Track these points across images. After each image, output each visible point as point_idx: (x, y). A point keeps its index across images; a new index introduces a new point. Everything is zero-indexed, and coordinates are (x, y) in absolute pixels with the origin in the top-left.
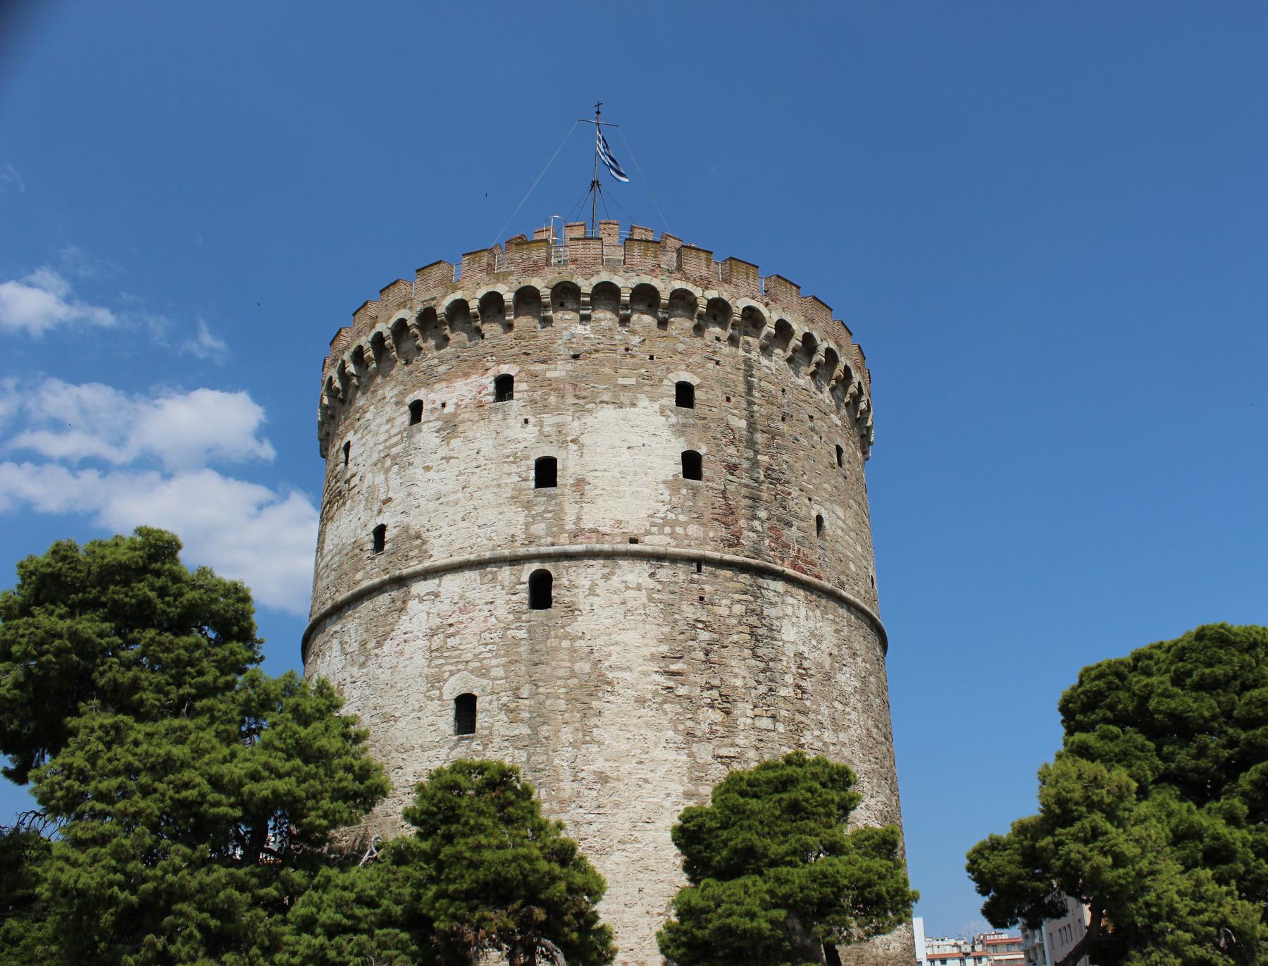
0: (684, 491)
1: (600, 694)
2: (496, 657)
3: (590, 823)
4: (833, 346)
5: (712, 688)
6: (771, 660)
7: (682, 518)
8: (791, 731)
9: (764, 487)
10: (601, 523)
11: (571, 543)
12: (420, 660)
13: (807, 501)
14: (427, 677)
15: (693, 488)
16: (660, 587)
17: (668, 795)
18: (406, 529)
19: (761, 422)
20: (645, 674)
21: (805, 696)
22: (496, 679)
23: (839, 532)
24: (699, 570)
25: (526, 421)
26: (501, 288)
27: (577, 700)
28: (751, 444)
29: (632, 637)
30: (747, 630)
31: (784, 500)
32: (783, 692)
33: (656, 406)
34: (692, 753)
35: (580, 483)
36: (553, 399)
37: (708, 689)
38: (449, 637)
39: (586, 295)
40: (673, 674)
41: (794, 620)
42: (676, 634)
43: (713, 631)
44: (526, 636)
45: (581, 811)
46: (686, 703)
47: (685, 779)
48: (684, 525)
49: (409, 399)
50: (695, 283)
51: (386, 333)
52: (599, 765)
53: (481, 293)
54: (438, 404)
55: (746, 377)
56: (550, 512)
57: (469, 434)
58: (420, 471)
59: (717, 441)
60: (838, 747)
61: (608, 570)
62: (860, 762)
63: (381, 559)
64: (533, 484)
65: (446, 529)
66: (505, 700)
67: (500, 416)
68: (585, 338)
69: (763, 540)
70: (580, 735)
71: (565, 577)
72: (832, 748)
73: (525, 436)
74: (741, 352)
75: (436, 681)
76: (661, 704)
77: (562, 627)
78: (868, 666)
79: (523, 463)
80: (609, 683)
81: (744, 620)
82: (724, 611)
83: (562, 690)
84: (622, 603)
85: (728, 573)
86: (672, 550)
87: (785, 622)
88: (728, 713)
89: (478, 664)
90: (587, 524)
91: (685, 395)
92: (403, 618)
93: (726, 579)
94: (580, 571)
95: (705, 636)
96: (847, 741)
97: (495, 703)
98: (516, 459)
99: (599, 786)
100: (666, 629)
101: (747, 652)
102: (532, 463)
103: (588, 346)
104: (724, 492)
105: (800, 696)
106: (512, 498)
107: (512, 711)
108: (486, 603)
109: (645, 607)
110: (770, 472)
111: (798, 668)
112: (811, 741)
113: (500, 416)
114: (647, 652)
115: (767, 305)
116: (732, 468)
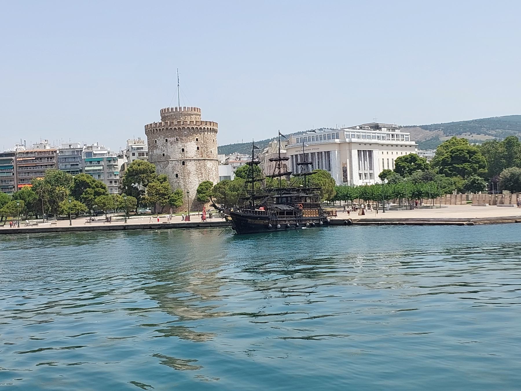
4: (213, 127)
12: (171, 170)
15: (198, 151)
26: (176, 127)
28: (204, 144)
29: (193, 168)
35: (187, 151)
36: (183, 141)
49: (166, 138)
51: (161, 129)
52: (190, 181)
53: (174, 127)
63: (164, 158)
71: (186, 162)
75: (173, 172)
91: (197, 140)
95: (200, 167)
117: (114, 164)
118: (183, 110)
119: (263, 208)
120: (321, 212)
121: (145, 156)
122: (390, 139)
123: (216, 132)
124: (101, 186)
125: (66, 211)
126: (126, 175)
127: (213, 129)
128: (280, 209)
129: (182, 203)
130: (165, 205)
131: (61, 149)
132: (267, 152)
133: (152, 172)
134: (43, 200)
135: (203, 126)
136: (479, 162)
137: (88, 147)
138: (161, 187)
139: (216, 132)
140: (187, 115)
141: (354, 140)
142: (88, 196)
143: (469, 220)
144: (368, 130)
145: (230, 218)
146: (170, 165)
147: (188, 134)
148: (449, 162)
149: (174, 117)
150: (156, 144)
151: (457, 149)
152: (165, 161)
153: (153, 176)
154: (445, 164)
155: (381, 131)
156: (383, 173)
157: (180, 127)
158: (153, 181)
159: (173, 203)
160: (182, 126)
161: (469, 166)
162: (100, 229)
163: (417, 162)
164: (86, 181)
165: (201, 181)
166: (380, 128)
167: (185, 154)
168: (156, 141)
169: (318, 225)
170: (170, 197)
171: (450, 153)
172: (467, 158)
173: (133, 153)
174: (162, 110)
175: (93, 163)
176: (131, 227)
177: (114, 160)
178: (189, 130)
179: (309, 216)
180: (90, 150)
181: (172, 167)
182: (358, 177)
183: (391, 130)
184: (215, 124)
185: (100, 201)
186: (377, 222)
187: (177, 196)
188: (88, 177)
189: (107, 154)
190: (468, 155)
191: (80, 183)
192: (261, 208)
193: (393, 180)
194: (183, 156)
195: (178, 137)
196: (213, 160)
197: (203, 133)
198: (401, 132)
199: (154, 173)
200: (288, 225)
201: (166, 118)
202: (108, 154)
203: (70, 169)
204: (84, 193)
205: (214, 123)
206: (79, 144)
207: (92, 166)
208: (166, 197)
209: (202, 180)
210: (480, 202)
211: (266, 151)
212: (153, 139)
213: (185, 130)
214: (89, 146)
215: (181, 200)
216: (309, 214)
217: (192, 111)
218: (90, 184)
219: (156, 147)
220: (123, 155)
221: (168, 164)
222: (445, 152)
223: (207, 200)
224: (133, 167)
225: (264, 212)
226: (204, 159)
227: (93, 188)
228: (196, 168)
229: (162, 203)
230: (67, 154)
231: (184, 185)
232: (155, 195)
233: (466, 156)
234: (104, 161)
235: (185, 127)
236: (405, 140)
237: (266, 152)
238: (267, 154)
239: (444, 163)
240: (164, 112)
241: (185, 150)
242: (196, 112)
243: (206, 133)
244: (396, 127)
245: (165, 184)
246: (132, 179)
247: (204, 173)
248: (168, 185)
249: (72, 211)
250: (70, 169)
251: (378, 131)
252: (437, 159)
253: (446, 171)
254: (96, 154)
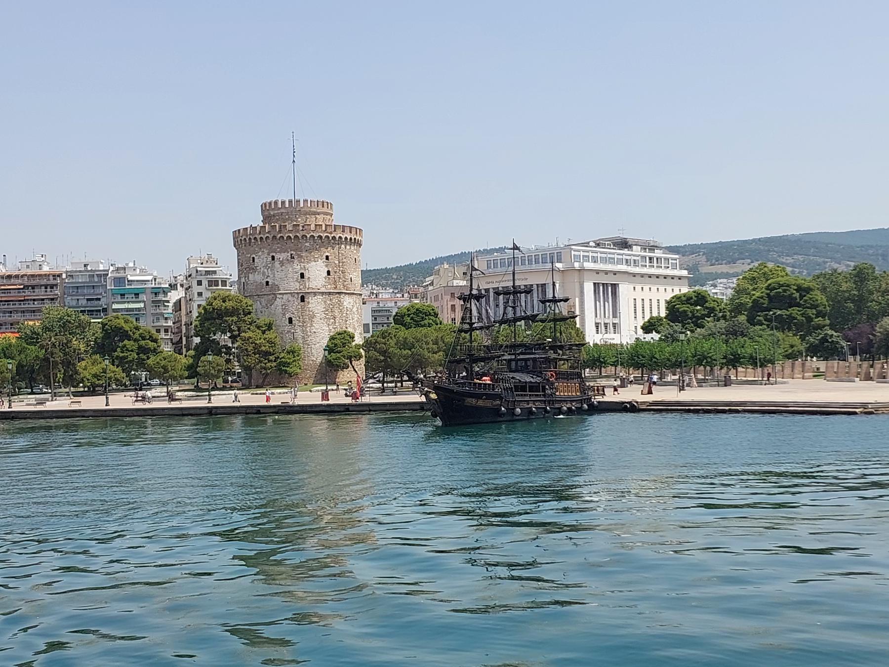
4: (355, 237)
12: (281, 310)
26: (291, 235)
35: (309, 278)
36: (303, 260)
49: (271, 254)
51: (264, 238)
52: (314, 330)
53: (287, 235)
63: (268, 288)
75: (284, 314)
91: (327, 258)
95: (331, 306)
116: (336, 272)
117: (163, 299)
118: (302, 205)
119: (488, 378)
120: (583, 389)
121: (220, 287)
122: (646, 266)
123: (358, 244)
124: (150, 337)
125: (88, 380)
126: (199, 318)
127: (355, 239)
128: (520, 381)
129: (300, 369)
130: (269, 371)
131: (70, 272)
132: (432, 284)
133: (248, 314)
134: (52, 359)
135: (337, 234)
136: (817, 306)
137: (118, 269)
138: (262, 340)
139: (358, 244)
140: (309, 215)
141: (588, 265)
142: (126, 354)
143: (864, 405)
144: (609, 248)
145: (433, 396)
146: (278, 302)
147: (312, 248)
148: (765, 306)
149: (287, 217)
150: (254, 264)
151: (779, 284)
152: (270, 294)
153: (249, 320)
154: (757, 309)
155: (632, 251)
156: (649, 321)
157: (298, 234)
158: (249, 329)
159: (284, 368)
160: (302, 233)
161: (799, 313)
162: (164, 413)
163: (707, 305)
164: (123, 327)
165: (333, 330)
166: (630, 246)
167: (305, 284)
168: (253, 258)
169: (580, 411)
170: (279, 357)
171: (766, 289)
172: (796, 299)
173: (198, 281)
174: (265, 204)
175: (126, 297)
176: (222, 411)
177: (164, 291)
178: (314, 240)
179: (566, 394)
180: (121, 274)
181: (282, 306)
182: (594, 329)
183: (647, 250)
184: (358, 230)
185: (157, 363)
186: (687, 408)
187: (291, 356)
188: (126, 322)
189: (152, 281)
190: (798, 294)
191: (113, 331)
192: (484, 378)
193: (669, 334)
194: (301, 287)
195: (294, 253)
196: (353, 294)
197: (338, 246)
198: (663, 253)
199: (250, 315)
200: (534, 409)
201: (273, 218)
202: (153, 282)
203: (85, 307)
204: (119, 350)
205: (356, 228)
206: (102, 263)
207: (125, 302)
208: (271, 358)
209: (335, 328)
210: (840, 375)
211: (430, 282)
212: (249, 255)
213: (306, 240)
214: (120, 266)
215: (298, 363)
216: (566, 391)
217: (318, 206)
218: (131, 333)
219: (254, 270)
220: (176, 285)
221: (275, 300)
222: (751, 288)
223: (344, 364)
224: (214, 304)
225: (489, 385)
226: (338, 293)
227: (136, 340)
228: (325, 308)
229: (265, 369)
230: (80, 281)
231: (303, 338)
232: (253, 355)
233: (794, 296)
234: (145, 295)
235: (307, 235)
236: (670, 268)
237: (430, 284)
238: (431, 288)
239: (757, 306)
240: (268, 208)
241: (306, 275)
242: (325, 210)
243: (343, 246)
244: (655, 245)
245: (270, 335)
246: (210, 325)
247: (339, 317)
248: (276, 337)
249: (98, 380)
250: (85, 307)
251: (626, 251)
252: (737, 301)
253: (760, 320)
254: (132, 281)
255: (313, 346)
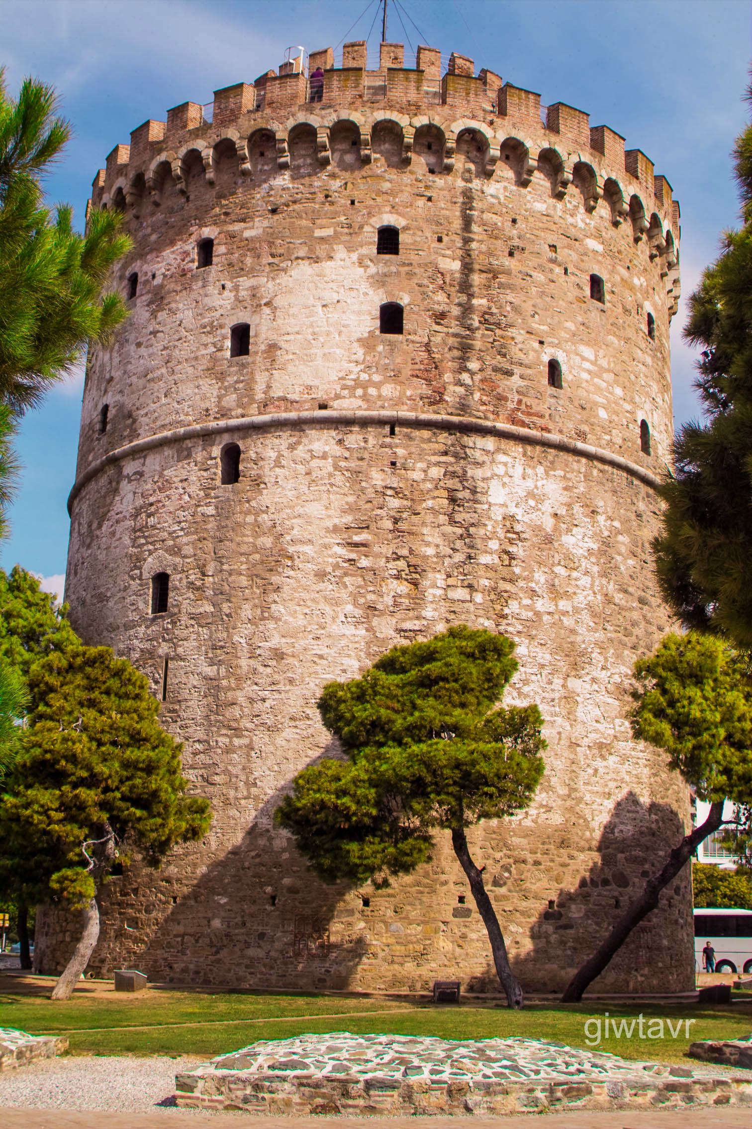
0: (380, 348)
1: (280, 570)
2: (186, 535)
3: (264, 700)
4: (586, 158)
5: (398, 558)
6: (473, 525)
7: (376, 378)
8: (492, 601)
9: (478, 334)
10: (290, 390)
11: (260, 413)
13: (536, 345)
14: (131, 556)
15: (391, 343)
16: (347, 454)
17: (344, 671)
18: (121, 407)
19: (479, 262)
20: (327, 546)
21: (514, 562)
22: (185, 557)
23: (585, 376)
24: (392, 433)
25: (223, 287)
27: (257, 576)
28: (465, 287)
29: (315, 509)
30: (445, 494)
31: (503, 346)
32: (484, 559)
33: (355, 256)
34: (372, 628)
35: (273, 347)
36: (249, 261)
37: (394, 560)
38: (149, 516)
39: (283, 141)
40: (356, 545)
41: (506, 480)
42: (362, 503)
43: (405, 497)
44: (214, 512)
45: (255, 687)
46: (370, 576)
47: (362, 654)
48: (378, 385)
49: (128, 274)
50: (401, 111)
52: (276, 641)
53: (183, 151)
54: (150, 274)
55: (463, 212)
56: (242, 382)
57: (173, 305)
58: (133, 347)
59: (421, 289)
60: (556, 617)
61: (294, 440)
62: (588, 631)
63: (104, 440)
64: (228, 354)
65: (153, 406)
66: (192, 577)
67: (200, 283)
68: (283, 189)
69: (472, 394)
70: (259, 611)
71: (251, 448)
72: (546, 618)
73: (222, 302)
74: (460, 183)
75: (137, 561)
76: (341, 577)
77: (248, 502)
78: (617, 524)
79: (219, 332)
80: (291, 558)
81: (442, 484)
82: (417, 475)
83: (244, 567)
84: (307, 474)
85: (426, 434)
86: (360, 413)
87: (494, 484)
88: (415, 584)
89: (171, 543)
90: (277, 393)
92: (117, 498)
93: (423, 440)
94: (268, 442)
95: (395, 503)
96: (570, 609)
97: (185, 581)
98: (212, 328)
99: (274, 663)
100: (351, 499)
101: (443, 519)
102: (228, 332)
103: (286, 197)
104: (427, 345)
105: (507, 563)
106: (208, 369)
107: (198, 589)
108: (181, 481)
109: (331, 475)
110: (487, 317)
111: (508, 531)
112: (517, 611)
113: (200, 283)
114: (329, 524)
115: (491, 123)
116: (440, 317)
157: (232, 134)
221: (116, 491)
255: (260, 739)
